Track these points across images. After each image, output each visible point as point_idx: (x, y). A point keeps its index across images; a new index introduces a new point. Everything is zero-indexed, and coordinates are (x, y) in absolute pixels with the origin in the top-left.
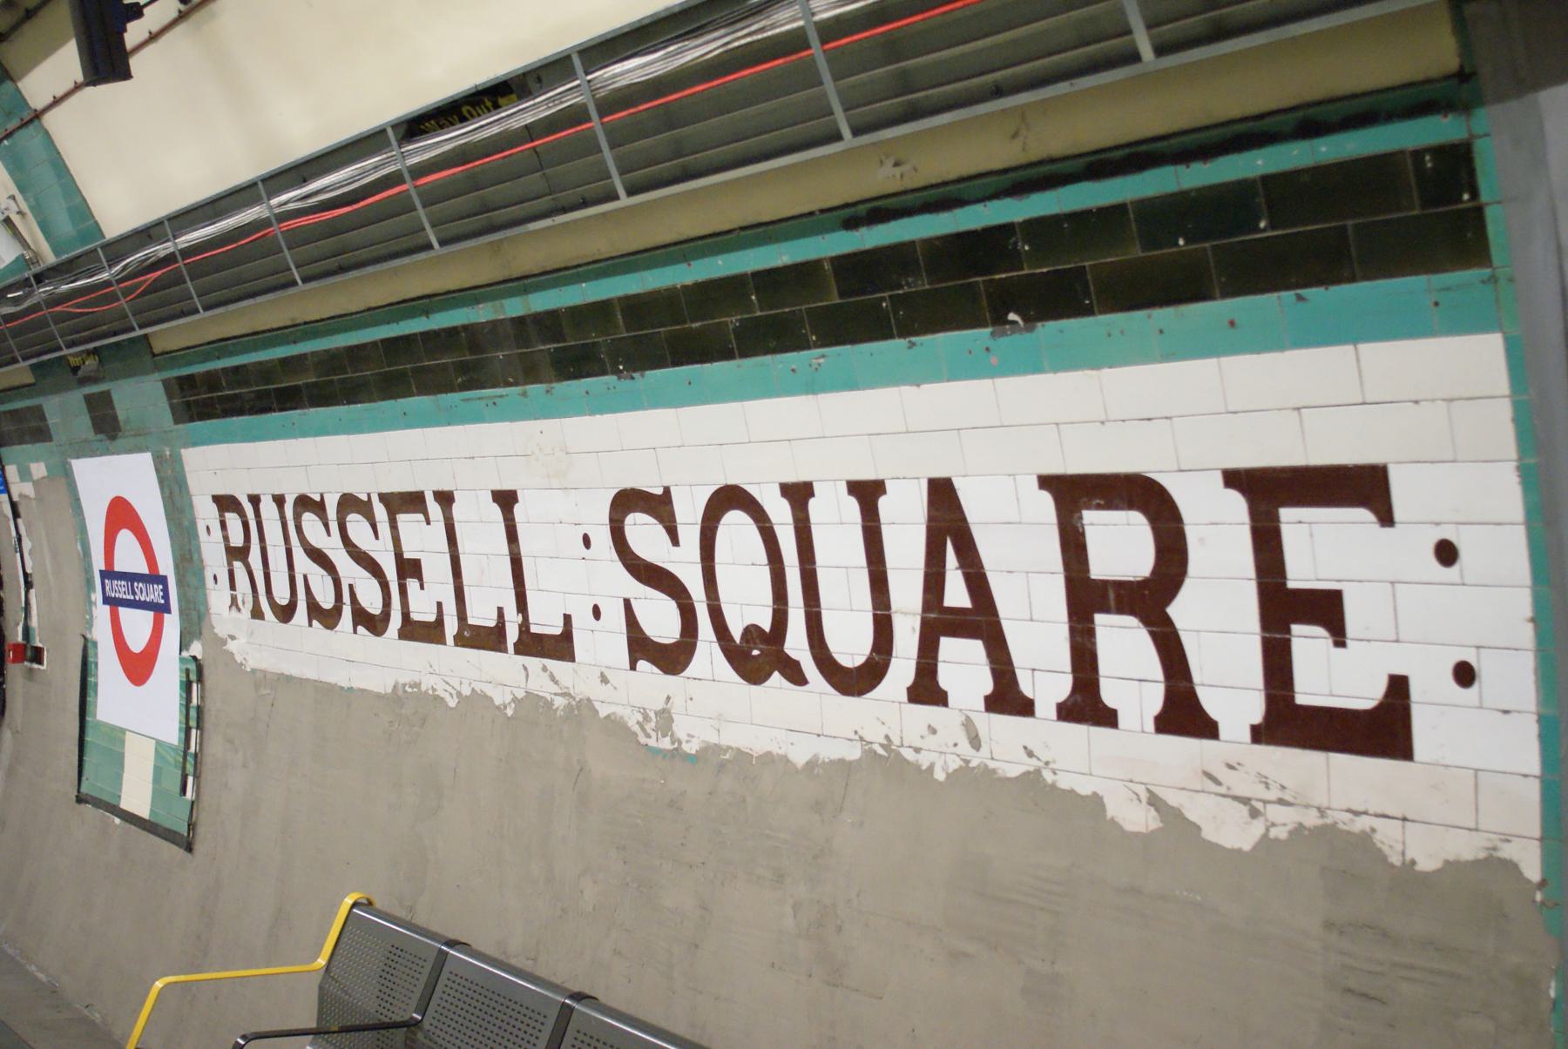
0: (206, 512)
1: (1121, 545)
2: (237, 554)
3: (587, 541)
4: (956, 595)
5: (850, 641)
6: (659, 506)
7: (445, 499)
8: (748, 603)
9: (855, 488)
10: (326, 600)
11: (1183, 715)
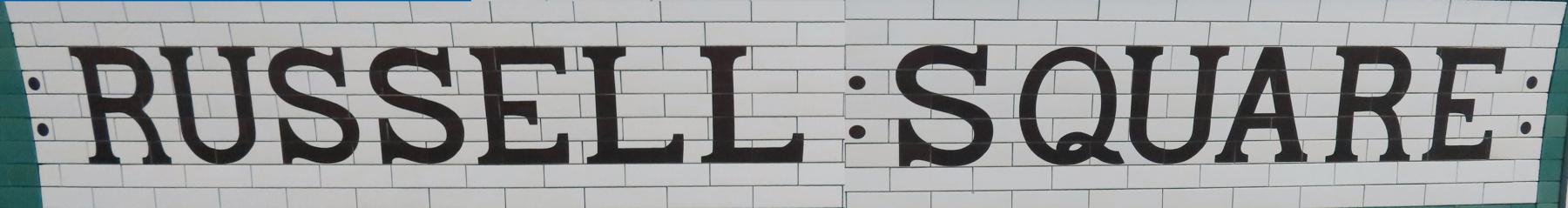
4: (1266, 105)
7: (604, 59)
11: (1395, 153)
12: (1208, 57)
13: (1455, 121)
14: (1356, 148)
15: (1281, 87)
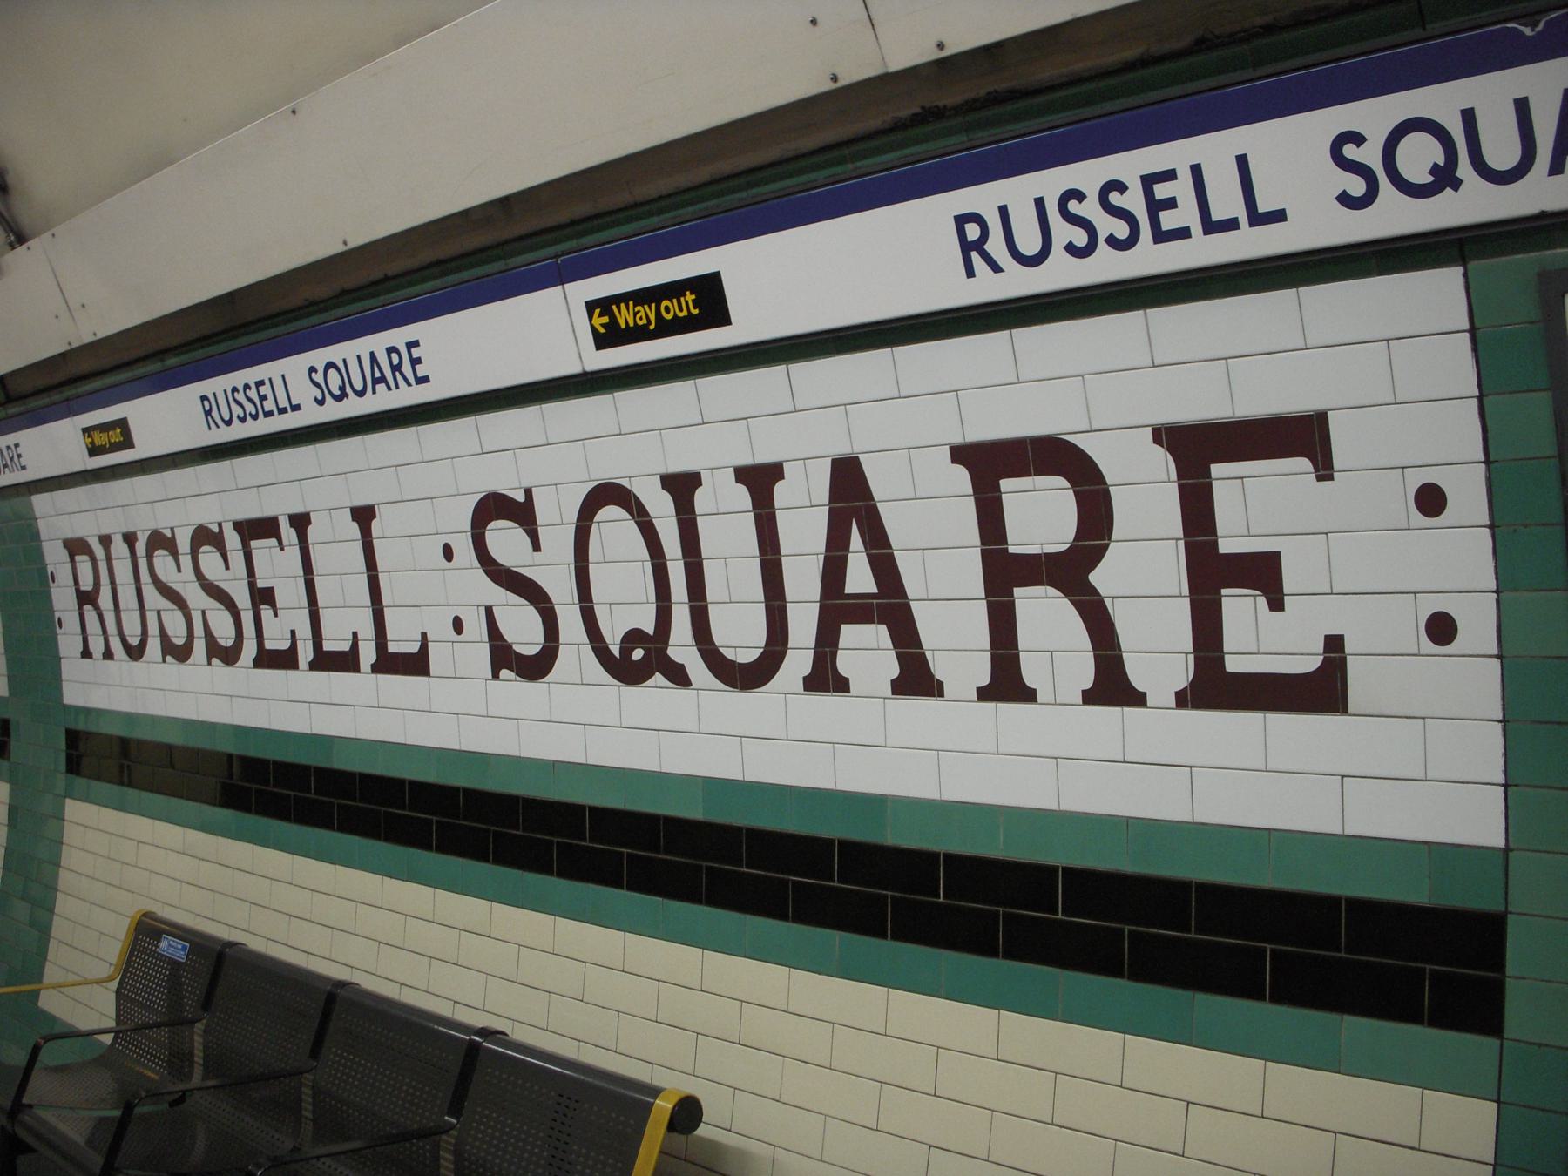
0: (54, 555)
1: (1040, 514)
2: (86, 598)
3: (448, 552)
4: (860, 578)
5: (741, 633)
6: (522, 513)
7: (301, 522)
8: (626, 604)
9: (744, 475)
10: (178, 636)
11: (1112, 687)
12: (760, 481)
13: (1240, 609)
14: (1032, 671)
15: (877, 538)
